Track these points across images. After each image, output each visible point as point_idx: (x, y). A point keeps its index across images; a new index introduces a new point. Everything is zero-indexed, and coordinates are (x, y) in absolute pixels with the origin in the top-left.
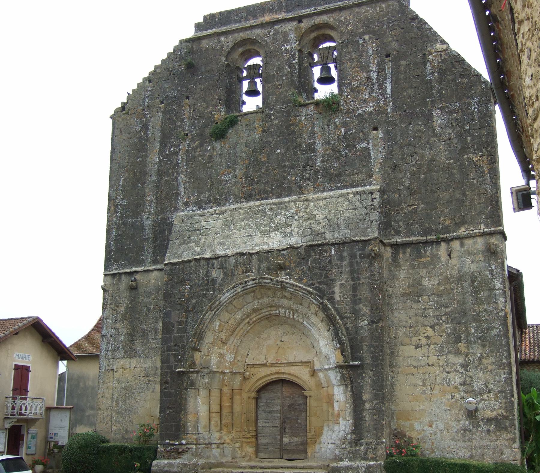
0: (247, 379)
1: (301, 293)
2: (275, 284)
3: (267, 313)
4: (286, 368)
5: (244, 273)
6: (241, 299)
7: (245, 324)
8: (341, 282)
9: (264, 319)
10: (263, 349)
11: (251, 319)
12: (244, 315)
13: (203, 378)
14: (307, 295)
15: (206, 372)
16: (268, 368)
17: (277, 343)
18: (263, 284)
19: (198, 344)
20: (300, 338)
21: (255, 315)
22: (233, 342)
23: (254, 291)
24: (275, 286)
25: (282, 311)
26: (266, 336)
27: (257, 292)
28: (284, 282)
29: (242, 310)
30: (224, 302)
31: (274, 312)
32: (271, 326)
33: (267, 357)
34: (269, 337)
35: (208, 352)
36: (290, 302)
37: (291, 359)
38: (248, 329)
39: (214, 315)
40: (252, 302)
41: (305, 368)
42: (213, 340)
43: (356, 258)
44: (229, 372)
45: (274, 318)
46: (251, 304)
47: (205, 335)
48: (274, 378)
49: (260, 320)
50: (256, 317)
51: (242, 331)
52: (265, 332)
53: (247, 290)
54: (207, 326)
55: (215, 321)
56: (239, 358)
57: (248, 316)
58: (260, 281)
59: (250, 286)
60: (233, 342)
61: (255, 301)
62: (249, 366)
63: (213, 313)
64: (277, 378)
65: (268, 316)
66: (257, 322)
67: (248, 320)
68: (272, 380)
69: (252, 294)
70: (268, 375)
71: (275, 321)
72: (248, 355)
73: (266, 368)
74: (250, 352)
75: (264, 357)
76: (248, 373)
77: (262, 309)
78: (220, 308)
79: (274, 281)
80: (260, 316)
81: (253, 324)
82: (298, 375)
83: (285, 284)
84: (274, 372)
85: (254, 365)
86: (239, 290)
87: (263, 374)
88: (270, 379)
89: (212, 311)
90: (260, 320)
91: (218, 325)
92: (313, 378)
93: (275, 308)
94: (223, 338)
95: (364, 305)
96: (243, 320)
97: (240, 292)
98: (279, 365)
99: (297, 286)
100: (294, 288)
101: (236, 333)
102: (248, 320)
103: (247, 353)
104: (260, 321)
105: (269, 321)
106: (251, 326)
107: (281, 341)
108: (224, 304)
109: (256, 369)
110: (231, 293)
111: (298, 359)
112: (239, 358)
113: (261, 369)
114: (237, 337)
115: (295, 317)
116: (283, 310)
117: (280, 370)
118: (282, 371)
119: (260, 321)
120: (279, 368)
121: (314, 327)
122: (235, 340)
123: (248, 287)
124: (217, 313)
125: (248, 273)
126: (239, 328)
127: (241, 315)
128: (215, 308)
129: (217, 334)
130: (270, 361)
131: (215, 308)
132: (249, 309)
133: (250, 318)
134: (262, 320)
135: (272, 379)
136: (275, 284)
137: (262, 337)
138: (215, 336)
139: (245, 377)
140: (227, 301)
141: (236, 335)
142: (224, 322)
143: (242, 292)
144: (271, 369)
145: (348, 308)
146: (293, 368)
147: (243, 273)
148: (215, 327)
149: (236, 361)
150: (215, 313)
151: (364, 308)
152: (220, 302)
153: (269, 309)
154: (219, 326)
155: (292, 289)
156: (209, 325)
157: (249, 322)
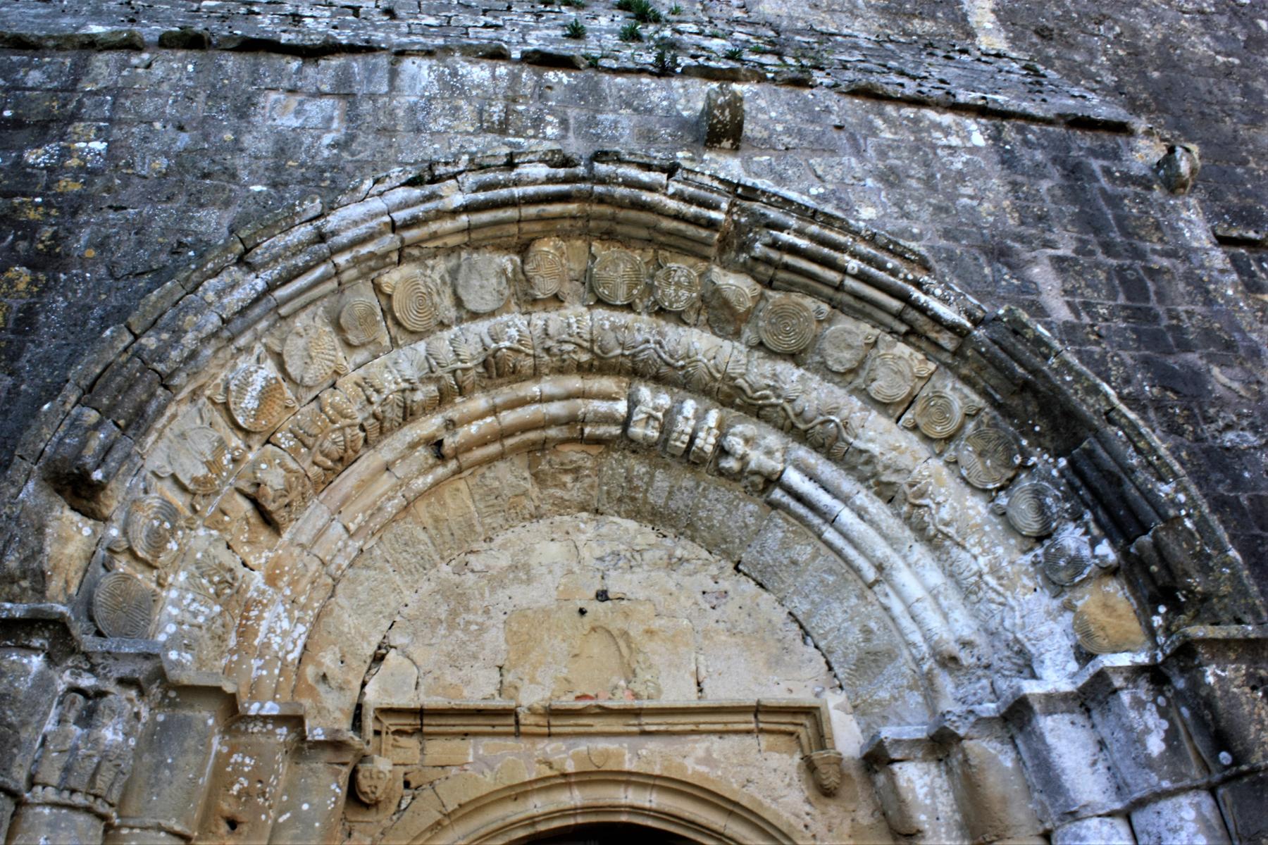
0: (367, 806)
1: (853, 265)
2: (690, 200)
3: (556, 409)
4: (651, 747)
5: (490, 130)
6: (441, 266)
7: (413, 446)
8: (1060, 252)
9: (516, 449)
10: (482, 629)
11: (451, 425)
12: (429, 378)
13: (88, 719)
14: (894, 273)
15: (125, 670)
16: (523, 744)
17: (580, 604)
18: (621, 191)
19: (107, 450)
20: (709, 585)
21: (480, 402)
22: (321, 533)
23: (523, 248)
24: (693, 209)
25: (652, 398)
26: (504, 561)
27: (546, 247)
28: (751, 193)
29: (421, 346)
30: (344, 238)
31: (602, 406)
32: (537, 516)
33: (509, 678)
34: (521, 571)
35: (157, 541)
36: (727, 344)
37: (678, 693)
38: (421, 483)
39: (256, 301)
40: (492, 314)
41: (771, 748)
42: (201, 471)
43: (1098, 180)
44: (279, 720)
45: (573, 454)
46: (482, 327)
47: (160, 411)
48: (563, 813)
49: (494, 449)
50: (482, 416)
51: (386, 482)
52: (498, 541)
53: (501, 214)
54: (193, 355)
55: (248, 349)
56: (329, 660)
57: (443, 399)
58: (602, 168)
59: (531, 190)
60: (321, 533)
61: (506, 317)
62: (390, 723)
63: (260, 285)
64: (586, 810)
65: (553, 432)
66: (479, 453)
67: (431, 425)
68: (542, 827)
69: (507, 261)
70: (520, 792)
71: (568, 478)
72: (378, 659)
73: (511, 742)
74: (398, 639)
75: (496, 676)
76: (383, 764)
77: (536, 374)
78: (307, 269)
79: (686, 181)
80: (509, 417)
81: (452, 465)
82: (731, 787)
83: (756, 206)
84: (570, 767)
85: (421, 713)
86: (458, 200)
87: (488, 782)
88: (532, 821)
89: (252, 268)
90: (494, 449)
91: (258, 381)
92: (833, 808)
93: (606, 383)
94: (274, 479)
95: (1211, 358)
96: (409, 414)
97: (455, 213)
98: (599, 724)
99: (829, 221)
100: (814, 229)
101: (349, 480)
102: (431, 425)
103: (376, 639)
104: (490, 461)
105: (535, 476)
106: (440, 471)
107: (602, 596)
108: (342, 259)
109: (438, 749)
110: (405, 205)
111: (718, 694)
112: (329, 660)
113: (472, 750)
114: (348, 511)
115: (735, 443)
116: (665, 400)
117: (607, 755)
118: (627, 767)
119: (490, 461)
120: (602, 744)
121: (863, 498)
122: (337, 529)
123: (518, 191)
124: (282, 293)
125: (517, 135)
126: (368, 462)
127: (409, 372)
128: (275, 259)
129: (236, 441)
130: (531, 696)
131: (275, 259)
132: (465, 352)
133: (452, 413)
134: (501, 456)
135: (549, 817)
136: (690, 200)
137: (476, 562)
138: (222, 445)
139: (364, 784)
140: (362, 241)
141: (346, 500)
142: (296, 383)
143: (464, 219)
144: (549, 747)
145: (1130, 361)
146: (699, 746)
147: (482, 130)
148: (242, 389)
149: (310, 671)
150: (271, 287)
151: (1216, 371)
152: (321, 237)
153: (575, 383)
154: (267, 395)
155: (800, 233)
156: (208, 352)
157: (436, 445)
